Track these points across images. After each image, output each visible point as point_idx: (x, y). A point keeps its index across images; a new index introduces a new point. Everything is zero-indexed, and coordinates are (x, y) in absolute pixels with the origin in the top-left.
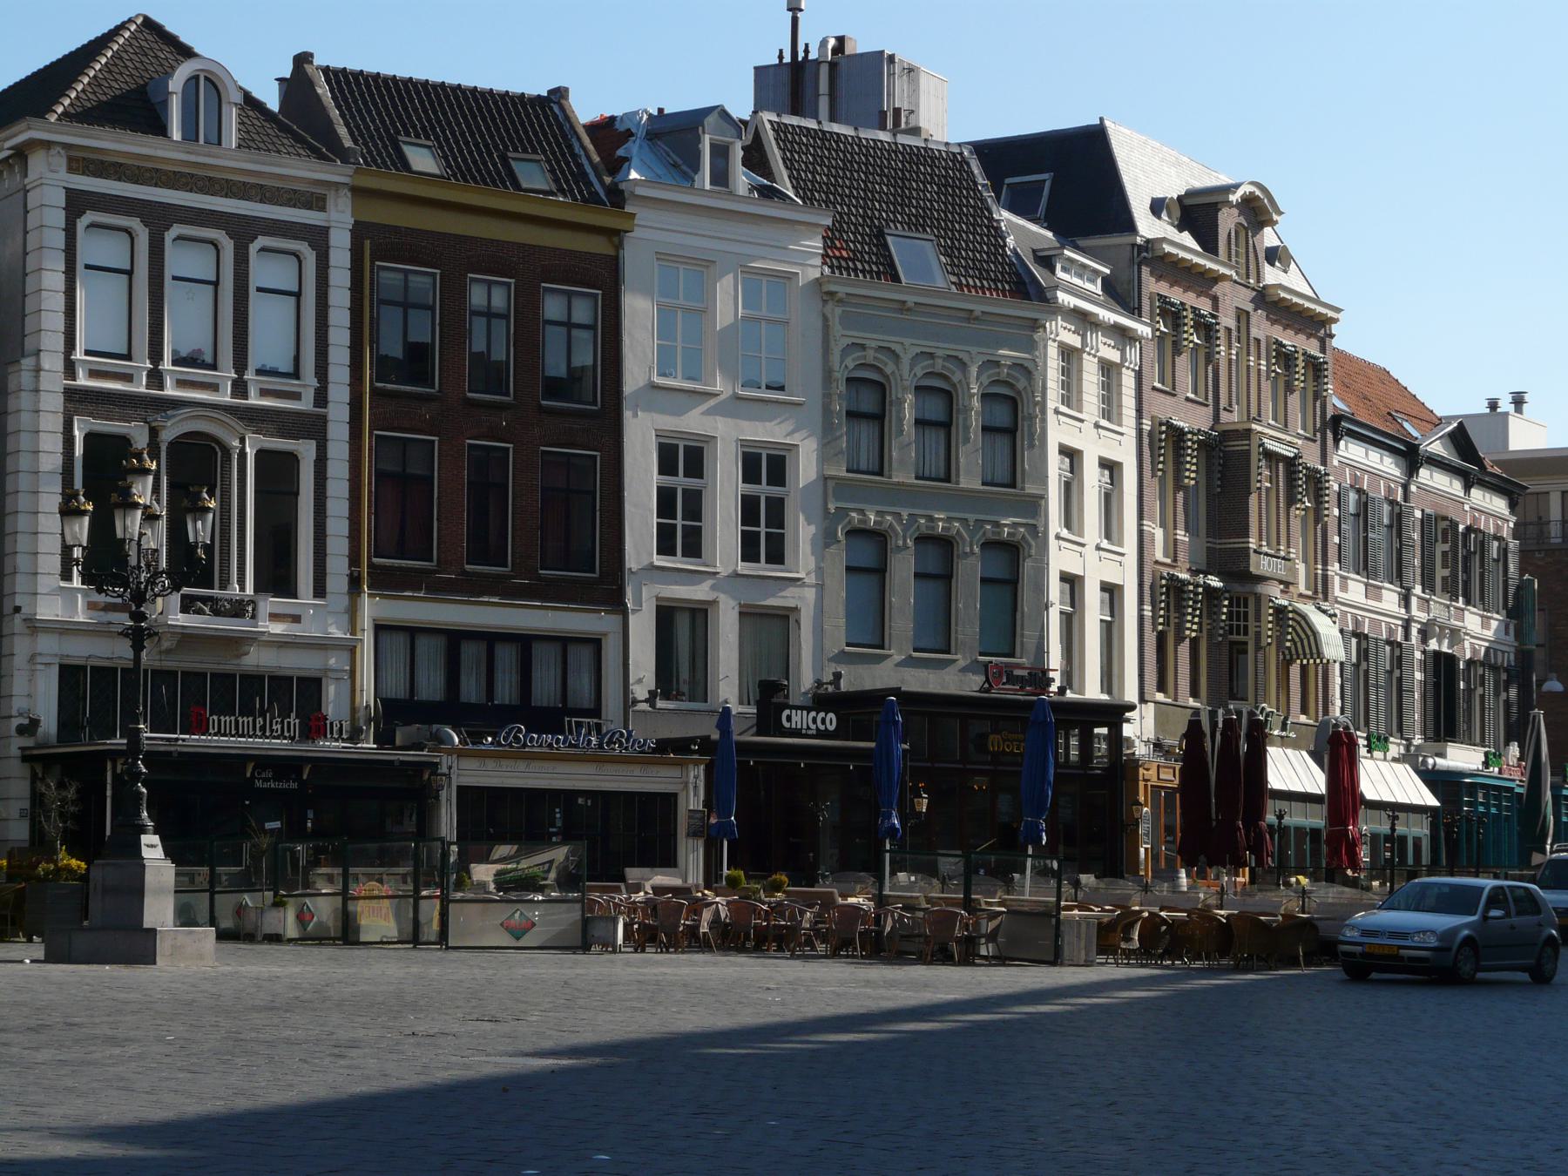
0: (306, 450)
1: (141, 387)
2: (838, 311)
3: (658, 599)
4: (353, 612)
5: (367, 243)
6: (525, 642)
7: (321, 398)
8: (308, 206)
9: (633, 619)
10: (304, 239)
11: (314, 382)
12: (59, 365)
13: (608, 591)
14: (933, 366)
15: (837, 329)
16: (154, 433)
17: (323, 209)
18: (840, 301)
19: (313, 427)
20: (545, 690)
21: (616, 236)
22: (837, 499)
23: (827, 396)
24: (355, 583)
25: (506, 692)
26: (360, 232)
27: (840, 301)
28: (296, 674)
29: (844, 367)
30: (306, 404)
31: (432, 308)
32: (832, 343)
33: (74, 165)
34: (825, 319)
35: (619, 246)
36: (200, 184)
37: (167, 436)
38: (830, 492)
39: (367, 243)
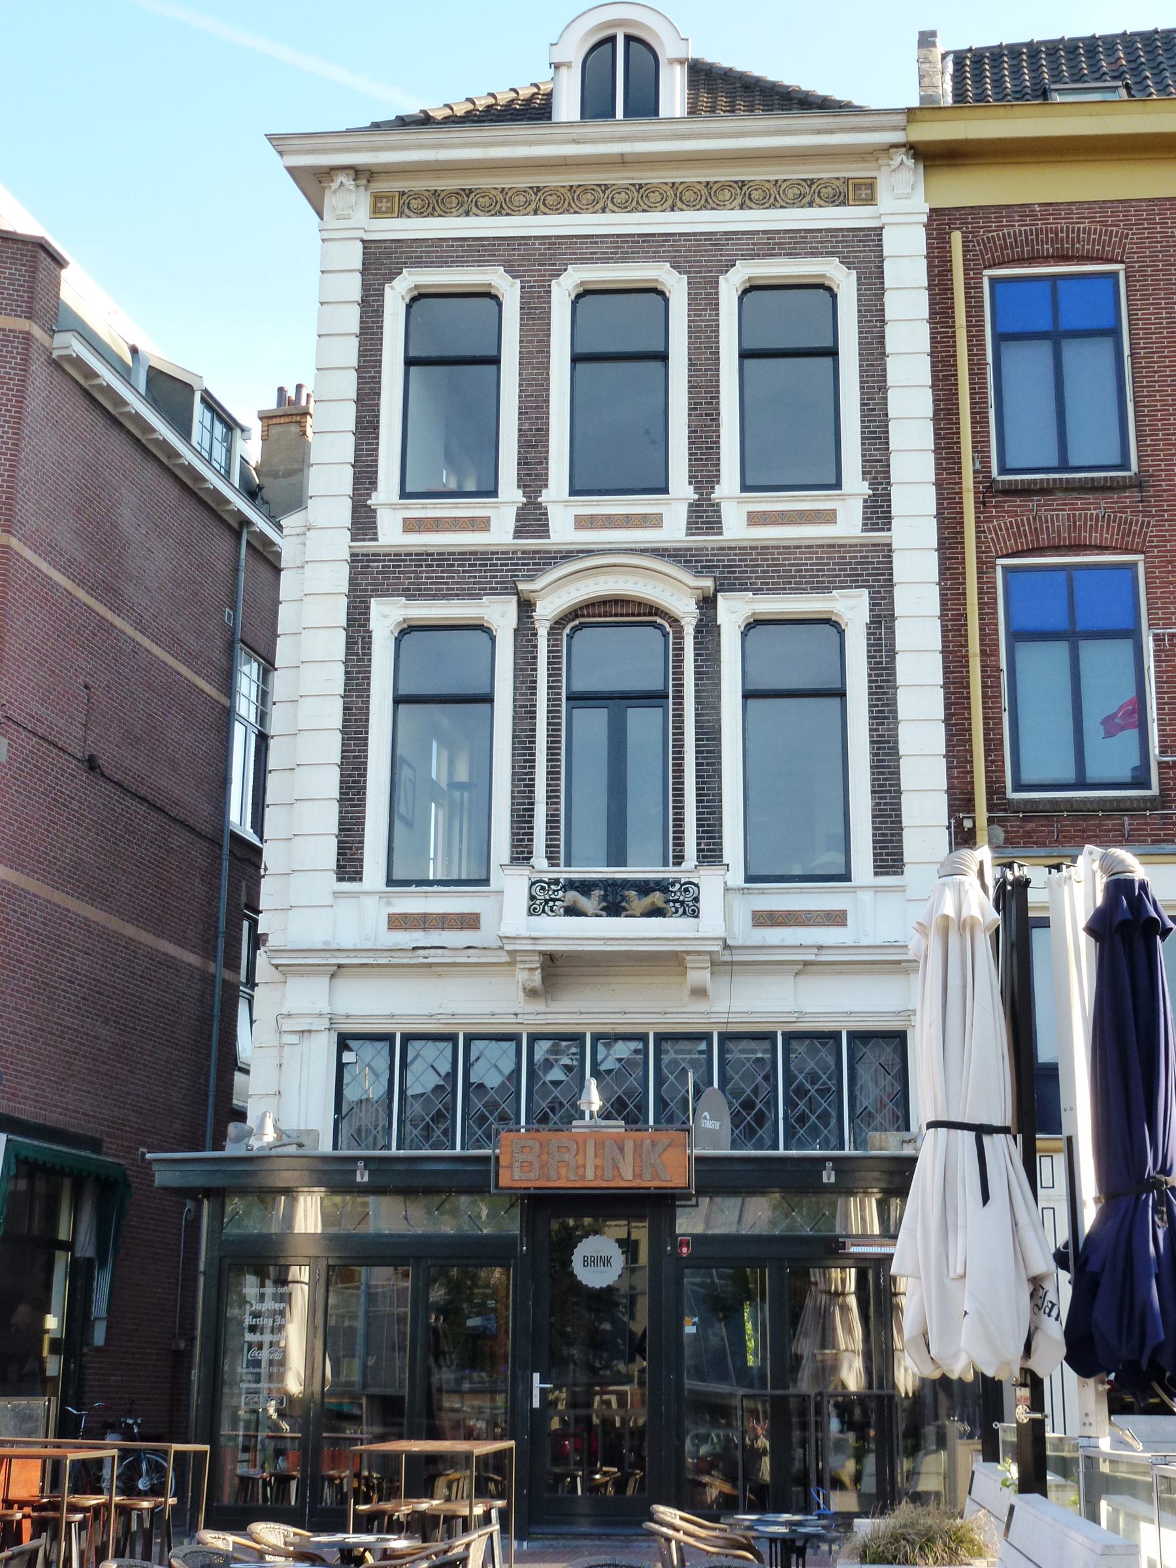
0: (852, 608)
1: (501, 532)
5: (957, 238)
7: (878, 511)
8: (839, 199)
10: (832, 254)
11: (865, 489)
12: (343, 513)
16: (526, 607)
17: (871, 200)
26: (940, 223)
28: (844, 1026)
30: (848, 523)
31: (1114, 332)
37: (547, 609)
39: (957, 238)
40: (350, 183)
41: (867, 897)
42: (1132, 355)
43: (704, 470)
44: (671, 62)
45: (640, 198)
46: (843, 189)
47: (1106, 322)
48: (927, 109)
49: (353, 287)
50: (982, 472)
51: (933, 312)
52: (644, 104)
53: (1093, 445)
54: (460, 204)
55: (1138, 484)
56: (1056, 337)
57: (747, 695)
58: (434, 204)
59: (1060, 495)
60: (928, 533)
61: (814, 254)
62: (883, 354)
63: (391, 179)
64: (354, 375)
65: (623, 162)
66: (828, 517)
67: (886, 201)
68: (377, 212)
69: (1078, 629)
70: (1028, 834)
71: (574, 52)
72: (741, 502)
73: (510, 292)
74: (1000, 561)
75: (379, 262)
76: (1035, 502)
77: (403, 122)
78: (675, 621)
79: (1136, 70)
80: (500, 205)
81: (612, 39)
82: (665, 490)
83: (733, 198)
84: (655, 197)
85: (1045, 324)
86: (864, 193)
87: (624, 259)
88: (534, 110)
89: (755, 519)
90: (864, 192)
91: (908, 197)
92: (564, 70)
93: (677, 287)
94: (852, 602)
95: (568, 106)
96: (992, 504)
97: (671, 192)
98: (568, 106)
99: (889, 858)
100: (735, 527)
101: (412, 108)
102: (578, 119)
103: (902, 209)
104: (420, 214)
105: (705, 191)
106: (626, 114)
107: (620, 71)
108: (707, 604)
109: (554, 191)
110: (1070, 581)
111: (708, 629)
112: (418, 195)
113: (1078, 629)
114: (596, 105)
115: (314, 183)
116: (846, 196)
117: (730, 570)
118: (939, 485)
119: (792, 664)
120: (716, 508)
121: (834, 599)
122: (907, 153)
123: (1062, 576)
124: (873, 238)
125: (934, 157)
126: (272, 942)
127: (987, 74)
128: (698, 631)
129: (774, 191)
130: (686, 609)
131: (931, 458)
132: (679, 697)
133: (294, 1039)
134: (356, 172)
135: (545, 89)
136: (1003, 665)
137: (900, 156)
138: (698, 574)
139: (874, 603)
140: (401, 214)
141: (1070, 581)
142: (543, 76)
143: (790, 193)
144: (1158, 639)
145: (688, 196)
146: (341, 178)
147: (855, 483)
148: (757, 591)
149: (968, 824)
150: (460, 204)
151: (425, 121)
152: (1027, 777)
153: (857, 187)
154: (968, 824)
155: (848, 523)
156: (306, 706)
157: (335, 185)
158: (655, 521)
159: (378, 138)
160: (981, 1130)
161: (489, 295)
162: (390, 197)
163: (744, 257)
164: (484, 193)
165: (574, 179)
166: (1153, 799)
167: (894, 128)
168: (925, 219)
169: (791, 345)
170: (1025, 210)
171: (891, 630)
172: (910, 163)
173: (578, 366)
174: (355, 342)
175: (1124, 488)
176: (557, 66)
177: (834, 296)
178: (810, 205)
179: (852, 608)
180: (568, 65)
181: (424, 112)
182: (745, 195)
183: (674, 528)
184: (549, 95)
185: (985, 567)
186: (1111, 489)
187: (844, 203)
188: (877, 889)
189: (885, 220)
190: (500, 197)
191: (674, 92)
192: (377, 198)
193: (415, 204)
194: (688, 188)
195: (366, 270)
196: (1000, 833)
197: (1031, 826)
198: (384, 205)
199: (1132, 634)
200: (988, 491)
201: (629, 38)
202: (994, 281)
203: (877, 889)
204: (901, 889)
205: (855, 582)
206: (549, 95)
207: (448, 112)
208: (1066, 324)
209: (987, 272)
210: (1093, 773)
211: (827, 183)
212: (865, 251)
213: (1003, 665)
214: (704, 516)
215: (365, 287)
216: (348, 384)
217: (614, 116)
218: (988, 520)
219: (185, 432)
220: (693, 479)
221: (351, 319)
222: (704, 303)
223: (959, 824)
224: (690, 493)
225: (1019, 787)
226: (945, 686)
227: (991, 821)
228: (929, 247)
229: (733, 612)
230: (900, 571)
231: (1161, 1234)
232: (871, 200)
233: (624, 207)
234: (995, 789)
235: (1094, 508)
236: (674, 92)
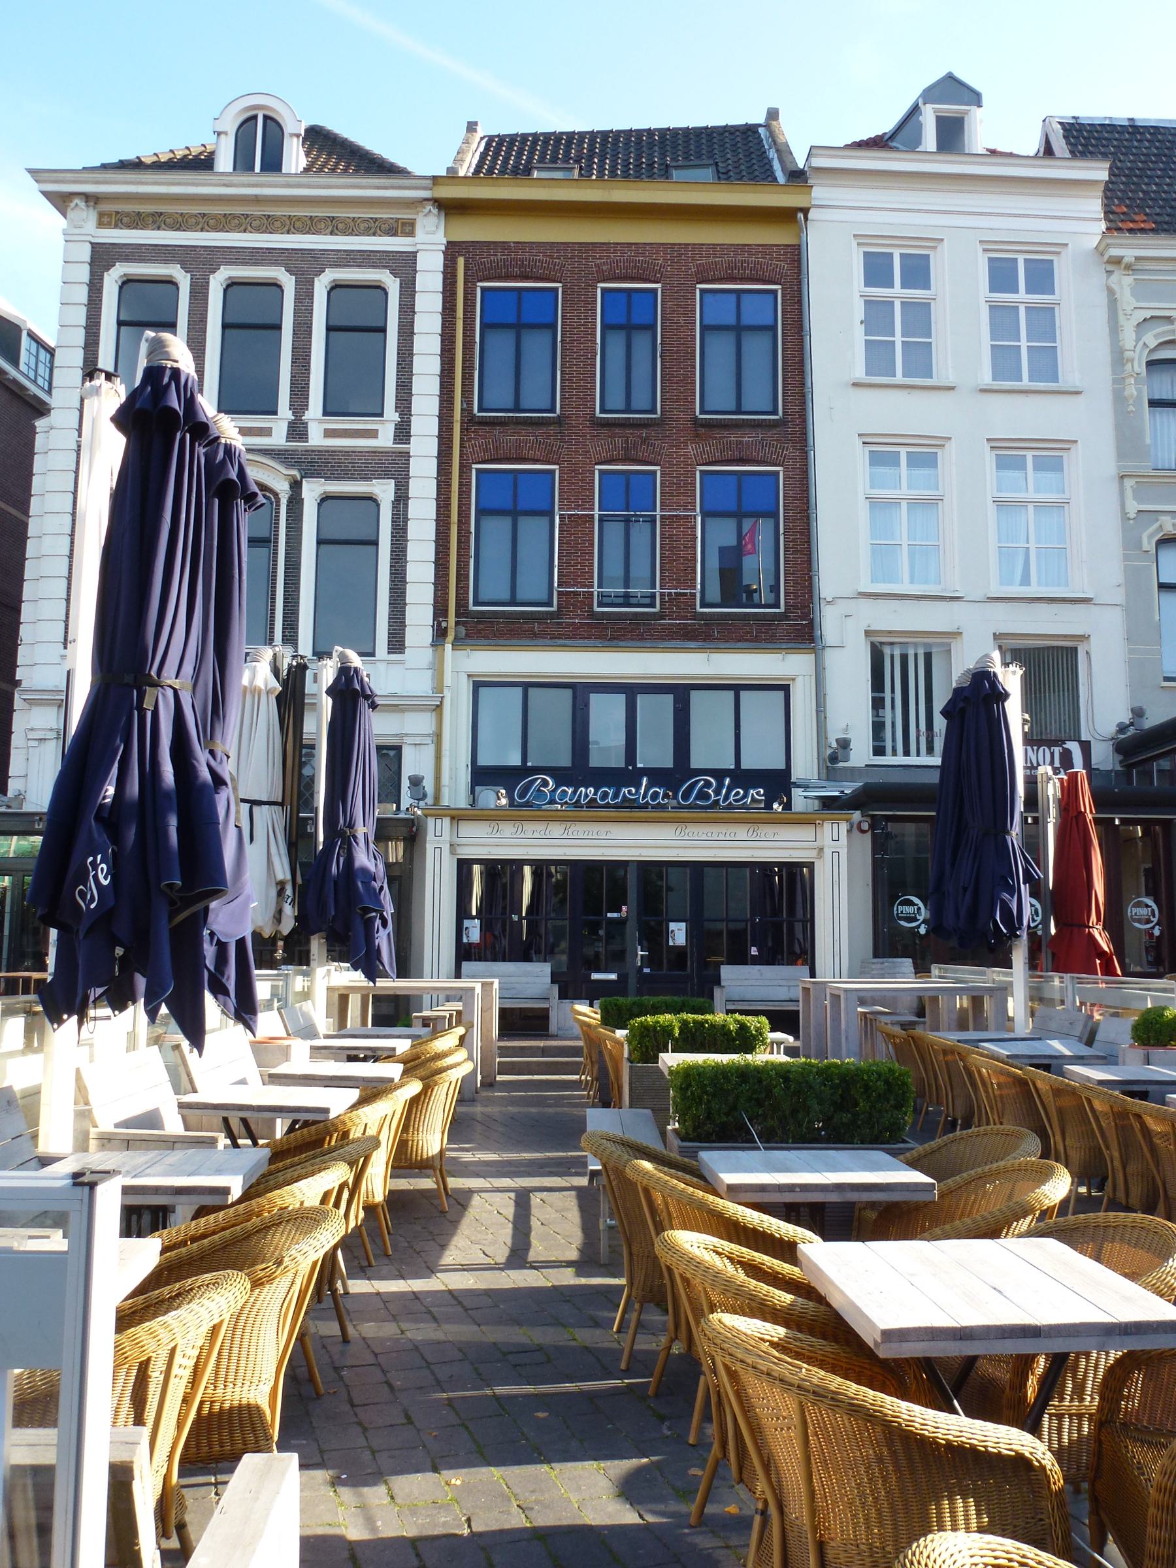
0: (384, 490)
2: (1128, 280)
3: (868, 633)
4: (438, 669)
5: (461, 261)
6: (681, 694)
7: (403, 432)
8: (392, 232)
9: (832, 659)
10: (385, 267)
11: (396, 417)
13: (798, 627)
15: (1127, 300)
17: (411, 234)
18: (1128, 267)
19: (396, 467)
20: (710, 749)
21: (791, 217)
22: (1140, 500)
23: (1119, 382)
24: (440, 634)
25: (656, 752)
26: (452, 250)
27: (1128, 267)
29: (1140, 347)
30: (385, 439)
32: (1121, 318)
33: (106, 220)
34: (1111, 292)
35: (800, 230)
36: (256, 223)
38: (1129, 493)
39: (461, 261)
40: (82, 204)
41: (382, 667)
42: (562, 341)
43: (299, 402)
44: (292, 135)
45: (268, 225)
46: (395, 225)
47: (548, 319)
48: (452, 176)
49: (84, 273)
50: (467, 410)
51: (444, 308)
52: (273, 163)
53: (535, 395)
54: (154, 222)
55: (558, 421)
56: (519, 327)
57: (320, 542)
58: (137, 221)
59: (512, 426)
60: (432, 447)
61: (374, 267)
62: (413, 333)
63: (111, 201)
64: (83, 331)
65: (257, 200)
66: (373, 434)
67: (421, 235)
68: (101, 224)
69: (519, 508)
70: (479, 632)
71: (230, 125)
72: (320, 421)
73: (184, 282)
74: (474, 466)
75: (102, 258)
76: (497, 431)
77: (123, 165)
78: (276, 494)
79: (590, 158)
80: (179, 224)
81: (255, 117)
82: (275, 413)
83: (326, 227)
84: (278, 224)
85: (512, 319)
86: (407, 229)
87: (256, 264)
88: (202, 163)
89: (329, 433)
90: (407, 228)
91: (434, 233)
92: (223, 136)
93: (289, 283)
94: (385, 487)
95: (225, 162)
96: (473, 432)
97: (288, 222)
98: (225, 162)
99: (397, 644)
100: (316, 438)
101: (130, 156)
102: (231, 170)
103: (429, 241)
104: (129, 227)
105: (309, 222)
106: (262, 170)
107: (259, 139)
108: (296, 486)
109: (214, 217)
110: (515, 480)
111: (296, 502)
112: (128, 215)
113: (519, 508)
114: (243, 161)
115: (61, 201)
116: (396, 231)
117: (310, 464)
118: (440, 417)
119: (348, 524)
120: (305, 425)
121: (373, 485)
122: (433, 205)
123: (511, 476)
124: (411, 257)
125: (451, 208)
126: (24, 685)
127: (511, 154)
128: (290, 501)
129: (352, 224)
130: (282, 487)
131: (437, 400)
132: (276, 542)
133: (35, 743)
134: (88, 197)
135: (209, 148)
136: (473, 530)
137: (429, 207)
138: (290, 466)
139: (398, 488)
140: (116, 227)
141: (515, 480)
142: (210, 141)
143: (362, 226)
144: (561, 517)
145: (298, 224)
146: (76, 201)
147: (391, 413)
148: (327, 478)
149: (444, 625)
150: (154, 222)
151: (136, 165)
152: (483, 597)
153: (403, 224)
154: (444, 625)
155: (385, 439)
156: (47, 540)
157: (72, 205)
158: (266, 432)
159: (110, 175)
160: (254, 803)
161: (171, 283)
162: (109, 215)
163: (331, 266)
164: (170, 215)
165: (228, 210)
166: (551, 613)
167: (425, 188)
168: (443, 248)
169: (358, 325)
170: (504, 245)
171: (406, 505)
172: (435, 211)
173: (227, 331)
174: (84, 309)
175: (550, 424)
176: (219, 134)
177: (386, 294)
178: (374, 235)
179: (384, 490)
180: (226, 133)
181: (138, 158)
182: (335, 227)
183: (279, 438)
184: (212, 153)
185: (464, 469)
186: (542, 424)
187: (395, 235)
188: (388, 662)
189: (419, 247)
190: (180, 219)
191: (295, 157)
192: (101, 215)
193: (125, 220)
194: (298, 220)
195: (92, 264)
196: (462, 630)
197: (481, 627)
198: (106, 220)
199: (550, 514)
200: (469, 421)
201: (266, 118)
202: (483, 289)
203: (388, 662)
204: (402, 662)
205: (385, 475)
206: (212, 153)
207: (155, 159)
208: (526, 319)
209: (480, 284)
210: (521, 595)
211: (385, 221)
212: (405, 266)
213: (473, 530)
214: (297, 430)
215: (92, 273)
216: (79, 337)
217: (253, 169)
218: (469, 440)
219: (15, 361)
220: (292, 406)
221: (82, 294)
222: (305, 295)
223: (439, 624)
224: (289, 415)
225: (476, 603)
226: (436, 541)
227: (457, 623)
228: (445, 266)
229: (312, 491)
230: (413, 470)
231: (342, 860)
232: (411, 234)
233: (258, 230)
234: (461, 604)
235: (529, 436)
236: (295, 157)
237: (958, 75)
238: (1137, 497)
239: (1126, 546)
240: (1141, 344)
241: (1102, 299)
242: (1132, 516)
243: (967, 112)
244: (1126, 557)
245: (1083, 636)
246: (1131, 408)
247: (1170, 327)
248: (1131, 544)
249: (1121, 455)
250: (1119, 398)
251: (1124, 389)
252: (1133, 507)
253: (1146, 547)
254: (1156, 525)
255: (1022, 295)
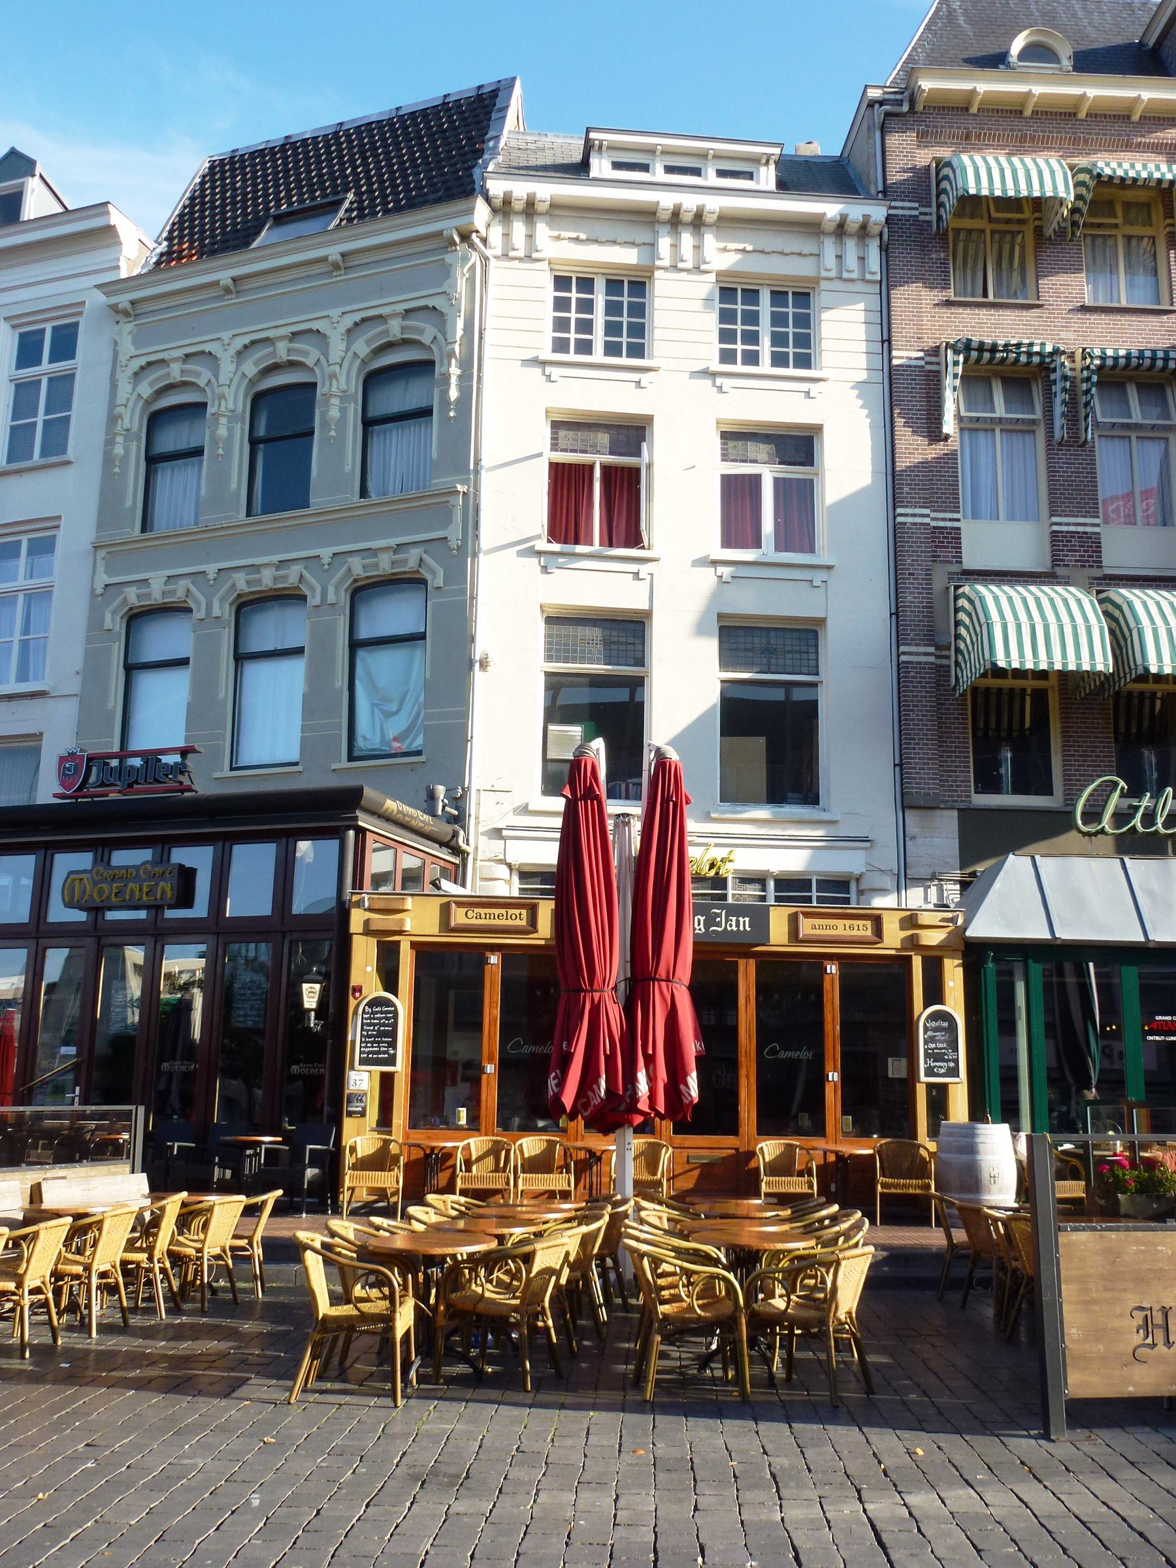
14: (274, 353)
18: (126, 313)
34: (116, 343)
38: (101, 566)
237: (20, 149)
238: (109, 571)
239: (89, 629)
240: (350, 354)
241: (107, 355)
242: (99, 591)
243: (22, 185)
244: (89, 640)
245: (34, 735)
246: (117, 470)
247: (164, 371)
248: (95, 624)
249: (101, 525)
250: (108, 460)
251: (327, 411)
252: (103, 578)
253: (108, 624)
254: (122, 597)
255: (45, 366)
